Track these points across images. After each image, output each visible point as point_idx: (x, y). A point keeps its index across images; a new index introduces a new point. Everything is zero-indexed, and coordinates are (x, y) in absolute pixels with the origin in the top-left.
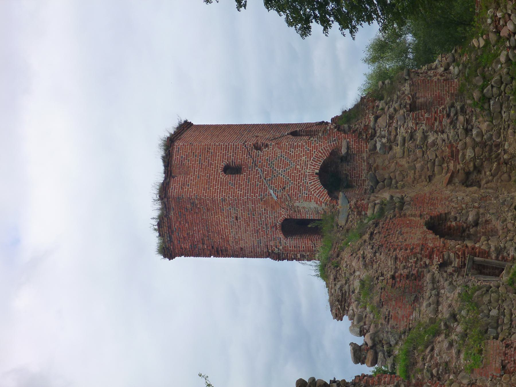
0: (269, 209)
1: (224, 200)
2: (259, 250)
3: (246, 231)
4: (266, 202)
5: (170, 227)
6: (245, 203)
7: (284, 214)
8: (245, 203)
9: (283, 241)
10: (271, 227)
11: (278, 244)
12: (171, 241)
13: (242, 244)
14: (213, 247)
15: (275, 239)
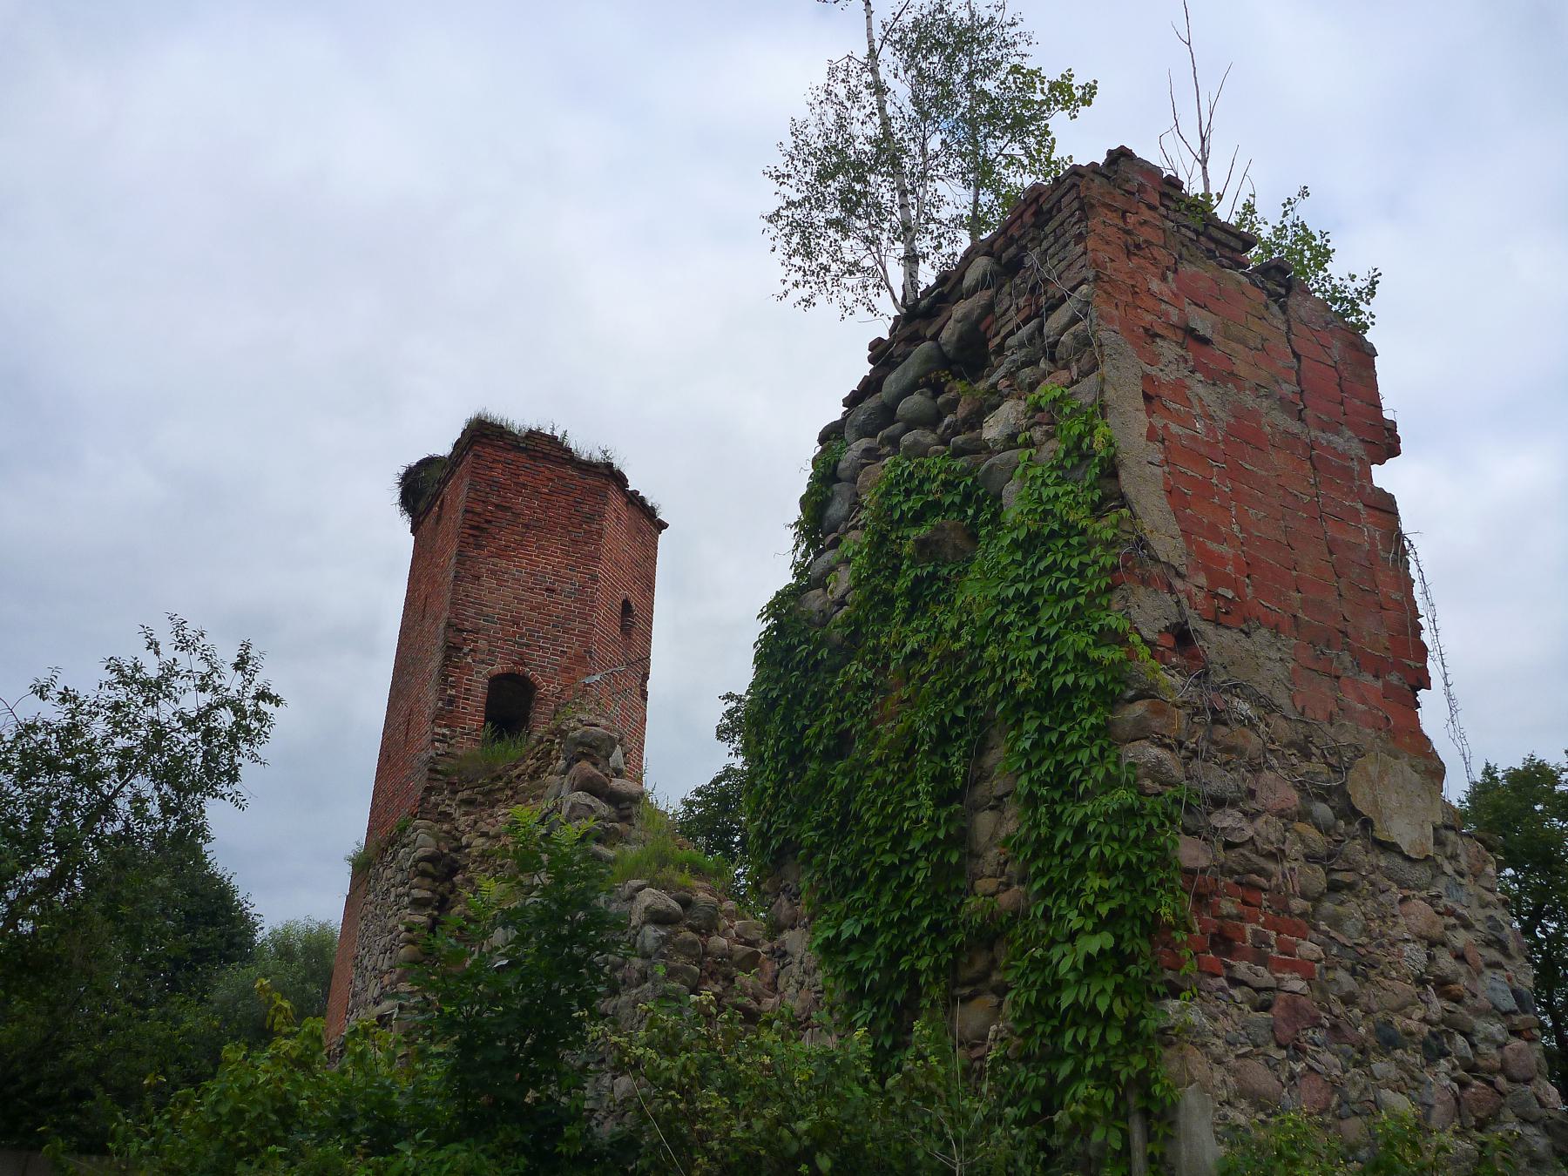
0: (565, 661)
1: (595, 579)
2: (471, 612)
3: (521, 601)
4: (580, 659)
5: (546, 457)
6: (584, 618)
7: (548, 687)
8: (584, 618)
9: (486, 670)
10: (521, 654)
11: (479, 656)
12: (517, 448)
13: (488, 582)
14: (488, 522)
15: (491, 653)
